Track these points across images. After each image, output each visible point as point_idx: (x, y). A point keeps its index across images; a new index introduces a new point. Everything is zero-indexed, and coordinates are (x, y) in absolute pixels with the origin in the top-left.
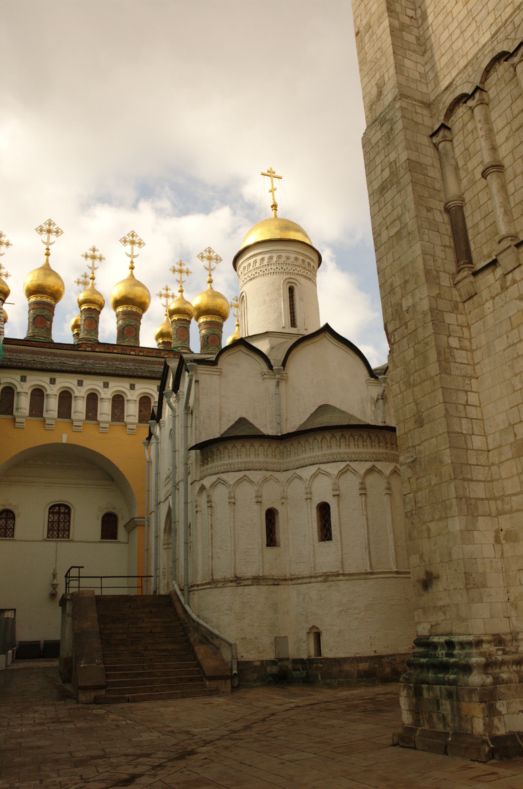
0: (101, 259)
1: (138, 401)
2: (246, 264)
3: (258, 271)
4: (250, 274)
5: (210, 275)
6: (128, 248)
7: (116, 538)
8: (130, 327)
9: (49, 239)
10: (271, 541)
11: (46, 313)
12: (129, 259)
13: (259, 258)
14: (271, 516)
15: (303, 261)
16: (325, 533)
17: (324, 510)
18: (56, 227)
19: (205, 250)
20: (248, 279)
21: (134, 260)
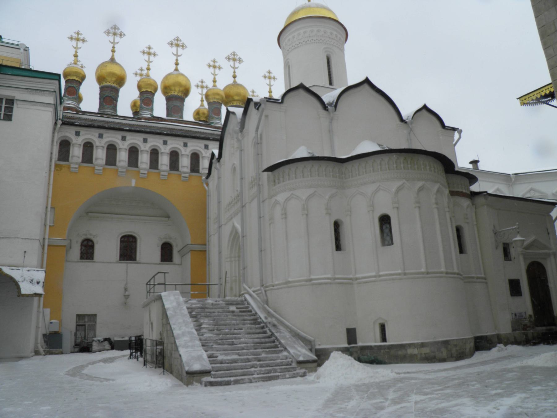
1: (190, 156)
2: (290, 37)
3: (302, 41)
4: (294, 44)
5: (234, 72)
6: (174, 49)
7: (172, 261)
9: (114, 39)
10: (338, 247)
11: (113, 94)
12: (175, 58)
13: (302, 31)
14: (337, 226)
15: (336, 36)
17: (385, 220)
18: (120, 31)
19: (231, 54)
20: (293, 48)
21: (179, 58)
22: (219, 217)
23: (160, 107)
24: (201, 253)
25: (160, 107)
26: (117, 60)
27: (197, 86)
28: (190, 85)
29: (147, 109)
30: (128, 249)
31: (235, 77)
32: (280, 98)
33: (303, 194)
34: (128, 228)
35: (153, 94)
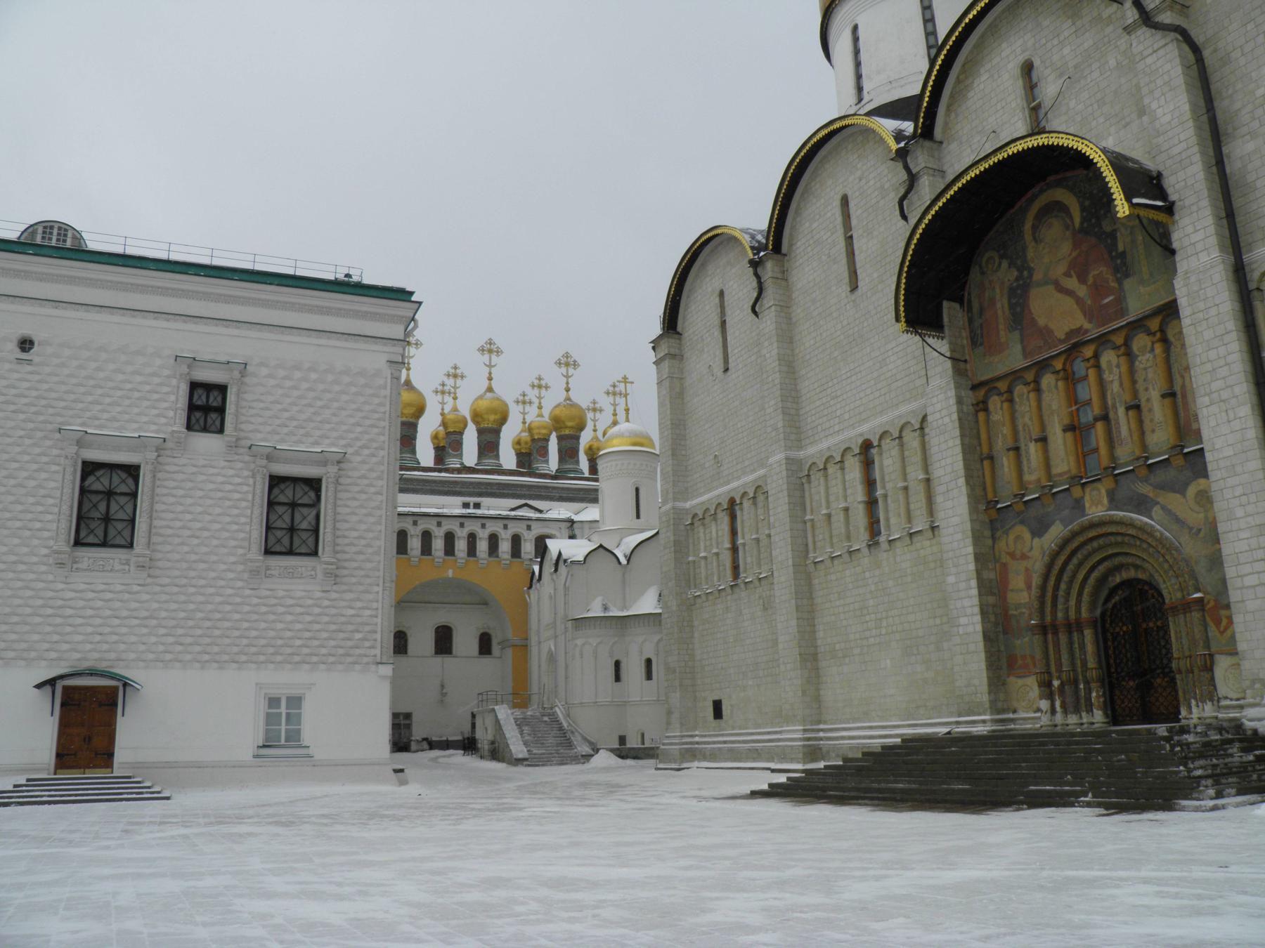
0: (462, 377)
6: (486, 358)
8: (489, 445)
12: (487, 369)
14: (617, 664)
16: (649, 676)
17: (649, 662)
22: (538, 631)
23: (470, 454)
24: (523, 648)
25: (470, 454)
26: (415, 383)
27: (518, 402)
28: (506, 405)
29: (455, 456)
30: (444, 641)
31: (568, 390)
32: (582, 559)
33: (594, 641)
34: (442, 617)
35: (461, 433)
